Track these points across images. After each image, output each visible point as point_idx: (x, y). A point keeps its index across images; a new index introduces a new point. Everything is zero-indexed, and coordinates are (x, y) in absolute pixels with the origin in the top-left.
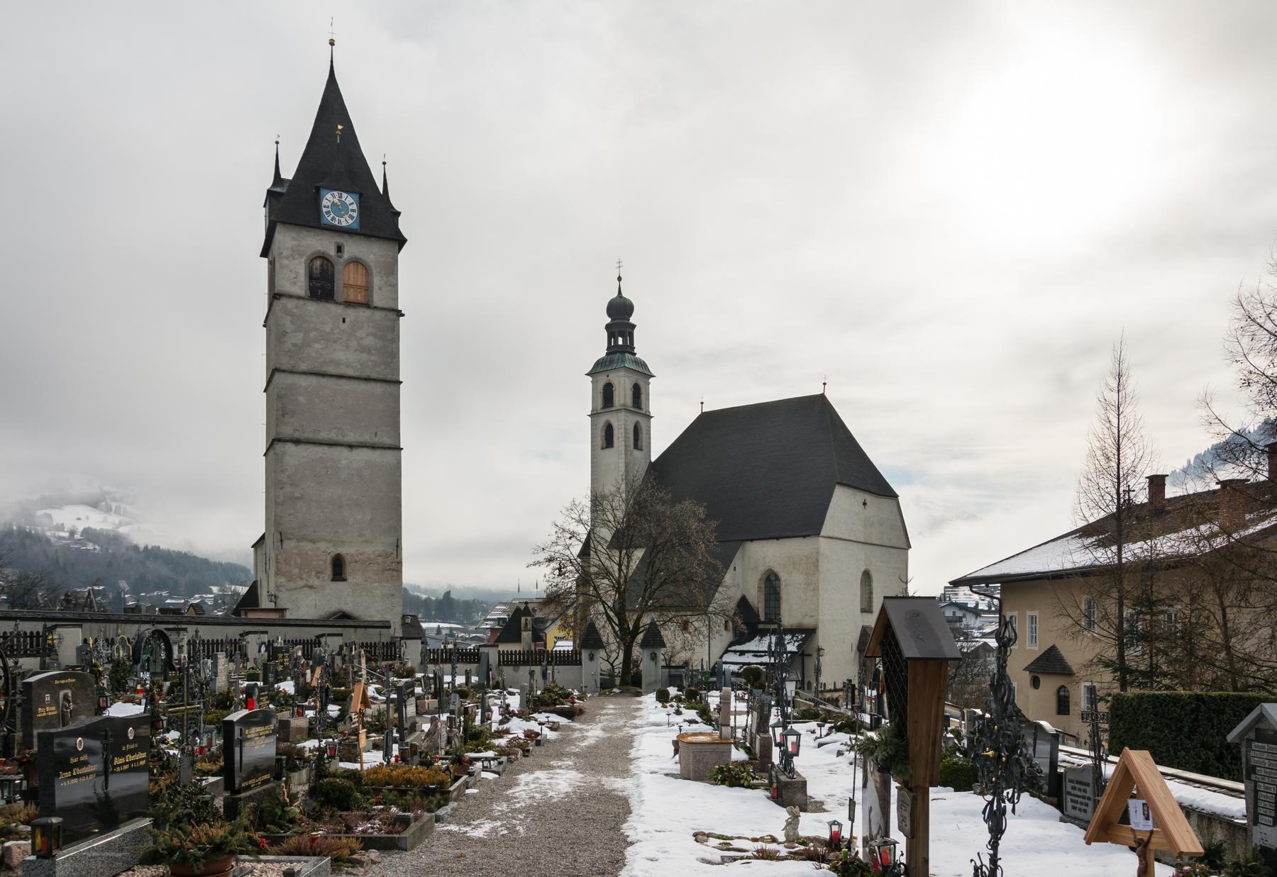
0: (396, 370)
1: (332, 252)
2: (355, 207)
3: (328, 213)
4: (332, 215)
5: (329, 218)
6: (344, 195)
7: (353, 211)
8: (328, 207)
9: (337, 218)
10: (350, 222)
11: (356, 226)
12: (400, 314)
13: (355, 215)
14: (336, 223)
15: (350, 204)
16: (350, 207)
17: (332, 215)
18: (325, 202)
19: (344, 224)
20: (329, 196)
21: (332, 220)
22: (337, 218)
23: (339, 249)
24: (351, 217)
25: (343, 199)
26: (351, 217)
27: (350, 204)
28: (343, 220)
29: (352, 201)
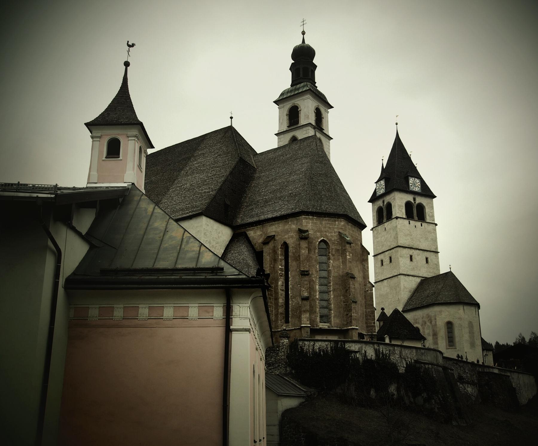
0: (437, 248)
1: (413, 202)
3: (411, 186)
4: (413, 187)
5: (412, 188)
9: (414, 188)
10: (419, 189)
11: (420, 191)
12: (436, 225)
13: (420, 186)
14: (414, 190)
17: (413, 187)
18: (410, 182)
19: (417, 190)
20: (411, 179)
21: (413, 188)
22: (414, 188)
23: (414, 199)
24: (419, 187)
25: (416, 181)
26: (419, 187)
28: (416, 188)
29: (418, 181)
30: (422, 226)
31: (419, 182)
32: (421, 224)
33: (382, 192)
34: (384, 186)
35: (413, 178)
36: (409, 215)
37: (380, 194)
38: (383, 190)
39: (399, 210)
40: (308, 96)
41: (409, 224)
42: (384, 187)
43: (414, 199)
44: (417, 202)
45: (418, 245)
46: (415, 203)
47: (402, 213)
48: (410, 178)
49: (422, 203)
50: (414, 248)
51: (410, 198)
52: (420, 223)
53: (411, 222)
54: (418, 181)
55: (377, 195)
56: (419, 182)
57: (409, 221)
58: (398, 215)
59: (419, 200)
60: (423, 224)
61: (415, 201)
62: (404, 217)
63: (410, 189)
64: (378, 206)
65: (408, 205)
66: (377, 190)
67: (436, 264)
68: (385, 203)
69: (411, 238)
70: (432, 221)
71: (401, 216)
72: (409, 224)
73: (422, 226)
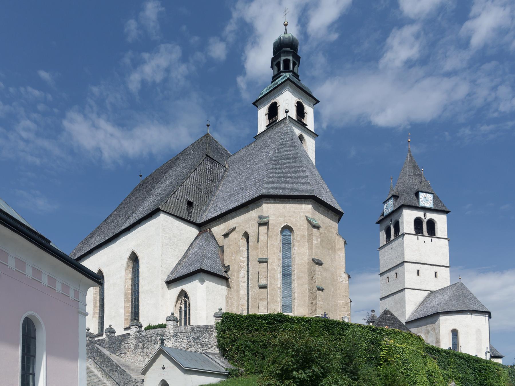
1: (423, 217)
2: (432, 199)
3: (422, 201)
5: (423, 203)
6: (428, 194)
7: (431, 200)
8: (422, 199)
10: (430, 204)
15: (430, 198)
16: (430, 199)
17: (424, 202)
24: (430, 203)
25: (427, 196)
26: (430, 203)
27: (430, 198)
30: (432, 241)
31: (431, 197)
32: (432, 239)
33: (389, 211)
34: (392, 204)
35: (425, 194)
37: (388, 213)
38: (391, 209)
40: (288, 88)
41: (418, 239)
42: (392, 205)
43: (425, 215)
44: (427, 219)
45: (426, 260)
46: (425, 218)
47: (410, 229)
48: (420, 193)
50: (422, 262)
51: (420, 214)
52: (430, 238)
53: (420, 237)
54: (430, 197)
55: (385, 215)
56: (431, 197)
57: (418, 237)
58: (405, 231)
59: (430, 216)
60: (433, 239)
61: (425, 217)
62: (413, 232)
64: (386, 226)
65: (418, 222)
66: (385, 210)
67: (446, 278)
68: (393, 221)
69: (419, 254)
70: (444, 236)
72: (418, 239)
73: (432, 241)
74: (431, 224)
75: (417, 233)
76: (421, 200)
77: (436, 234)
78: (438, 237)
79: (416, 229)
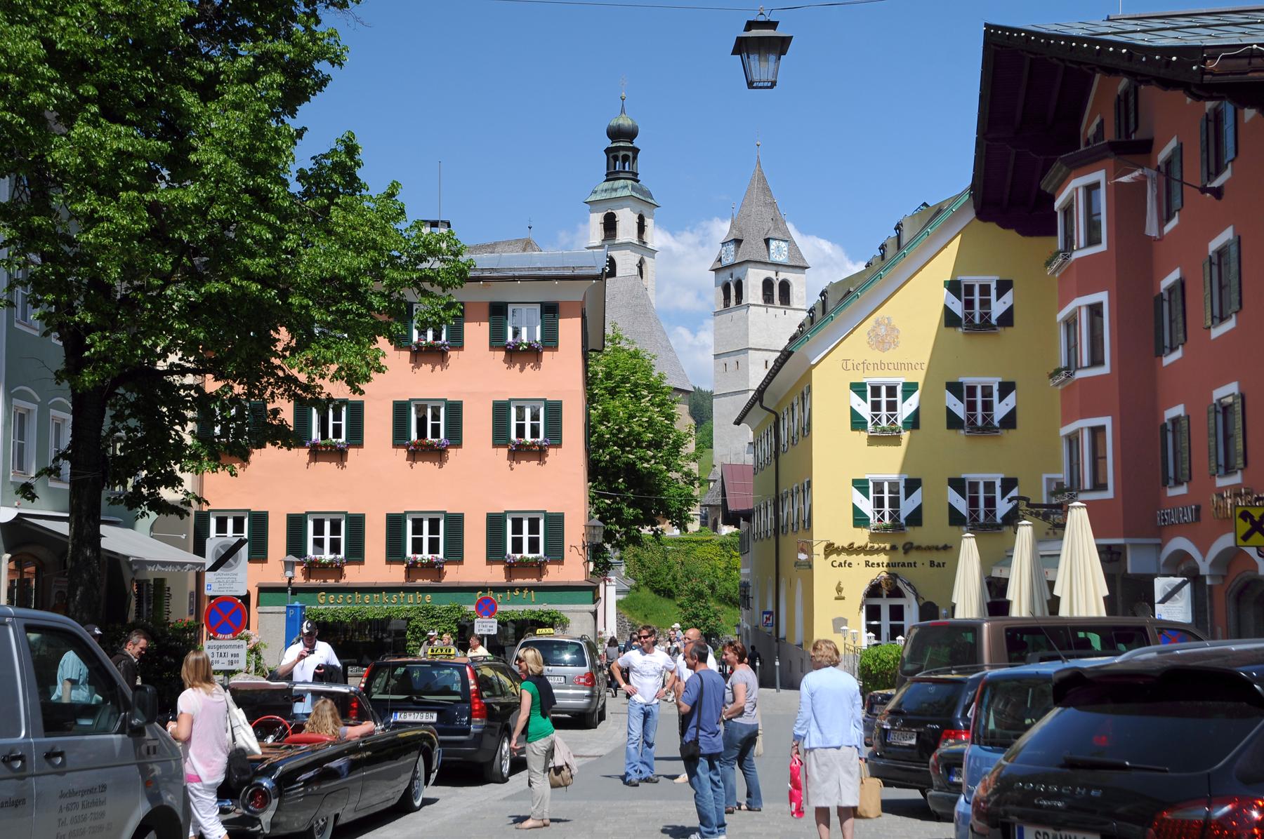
1: (774, 278)
2: (786, 249)
6: (781, 242)
35: (777, 242)
36: (768, 297)
39: (753, 292)
44: (780, 280)
49: (788, 278)
51: (771, 274)
58: (750, 302)
60: (787, 311)
62: (761, 302)
63: (771, 259)
65: (768, 284)
71: (756, 303)
74: (785, 287)
75: (765, 302)
76: (772, 251)
77: (791, 303)
78: (795, 306)
79: (764, 293)
